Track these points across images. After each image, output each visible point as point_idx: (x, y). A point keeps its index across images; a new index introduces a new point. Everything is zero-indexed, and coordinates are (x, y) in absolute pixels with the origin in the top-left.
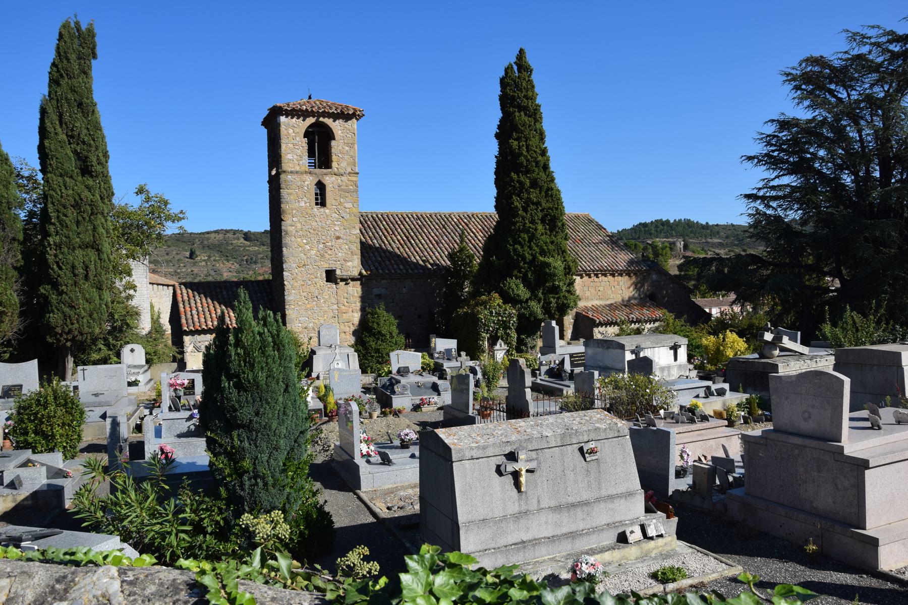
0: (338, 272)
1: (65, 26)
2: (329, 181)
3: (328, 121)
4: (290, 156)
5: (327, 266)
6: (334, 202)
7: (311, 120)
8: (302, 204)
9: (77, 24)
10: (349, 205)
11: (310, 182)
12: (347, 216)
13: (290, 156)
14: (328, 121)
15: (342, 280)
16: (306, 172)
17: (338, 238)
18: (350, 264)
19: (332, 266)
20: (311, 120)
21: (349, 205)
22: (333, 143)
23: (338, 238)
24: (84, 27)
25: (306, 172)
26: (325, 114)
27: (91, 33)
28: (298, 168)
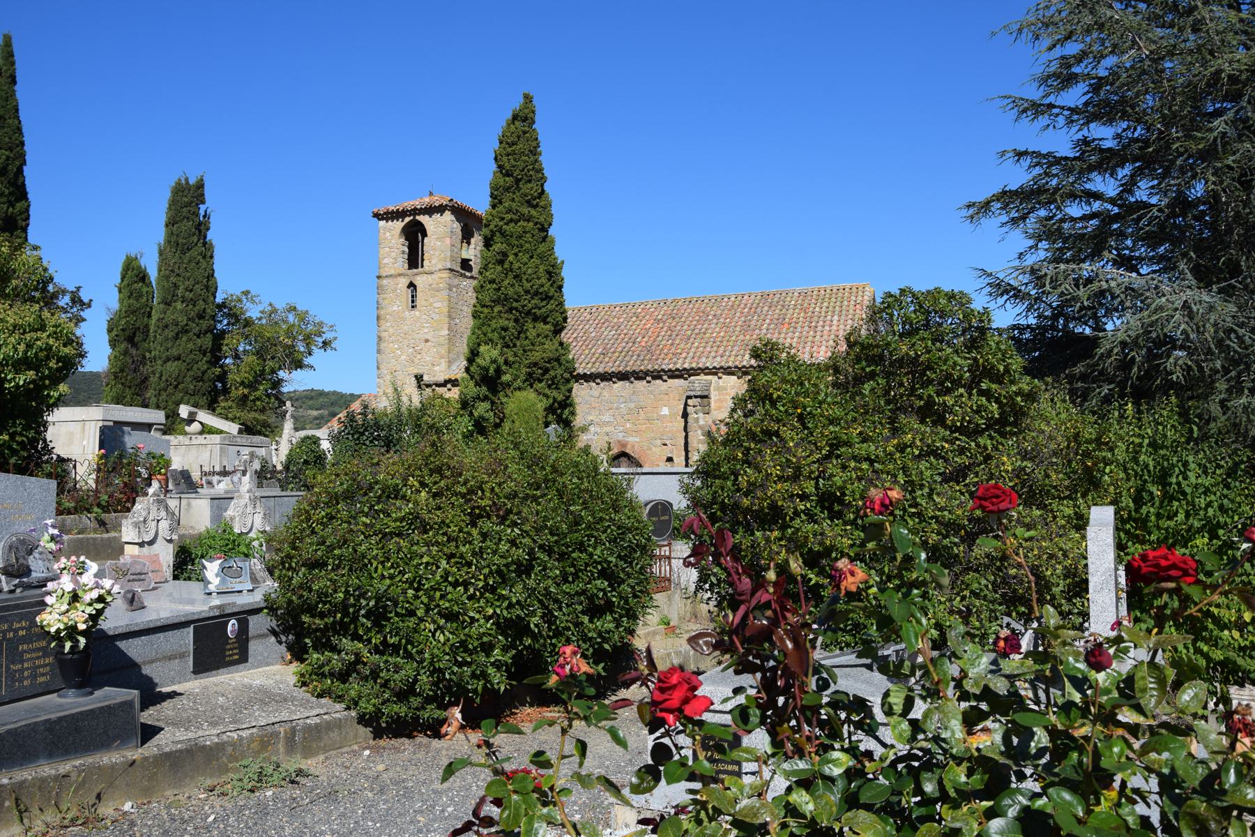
0: (425, 378)
1: (179, 183)
2: (420, 281)
3: (420, 218)
4: (386, 261)
5: (416, 371)
6: (424, 303)
7: (407, 219)
8: (395, 308)
9: (187, 180)
10: (439, 305)
11: (404, 282)
12: (436, 317)
13: (386, 261)
14: (420, 218)
15: (428, 386)
16: (400, 275)
17: (427, 341)
18: (437, 368)
19: (420, 372)
20: (407, 219)
21: (439, 305)
22: (426, 240)
23: (427, 341)
24: (192, 181)
25: (400, 275)
26: (415, 211)
27: (200, 185)
28: (392, 272)
